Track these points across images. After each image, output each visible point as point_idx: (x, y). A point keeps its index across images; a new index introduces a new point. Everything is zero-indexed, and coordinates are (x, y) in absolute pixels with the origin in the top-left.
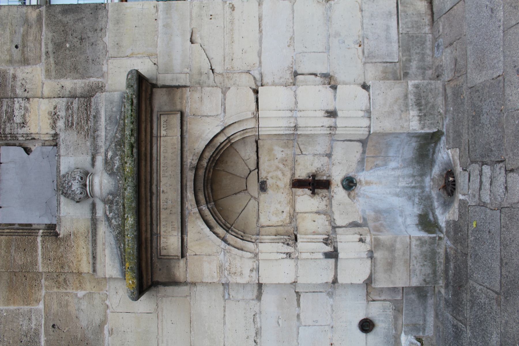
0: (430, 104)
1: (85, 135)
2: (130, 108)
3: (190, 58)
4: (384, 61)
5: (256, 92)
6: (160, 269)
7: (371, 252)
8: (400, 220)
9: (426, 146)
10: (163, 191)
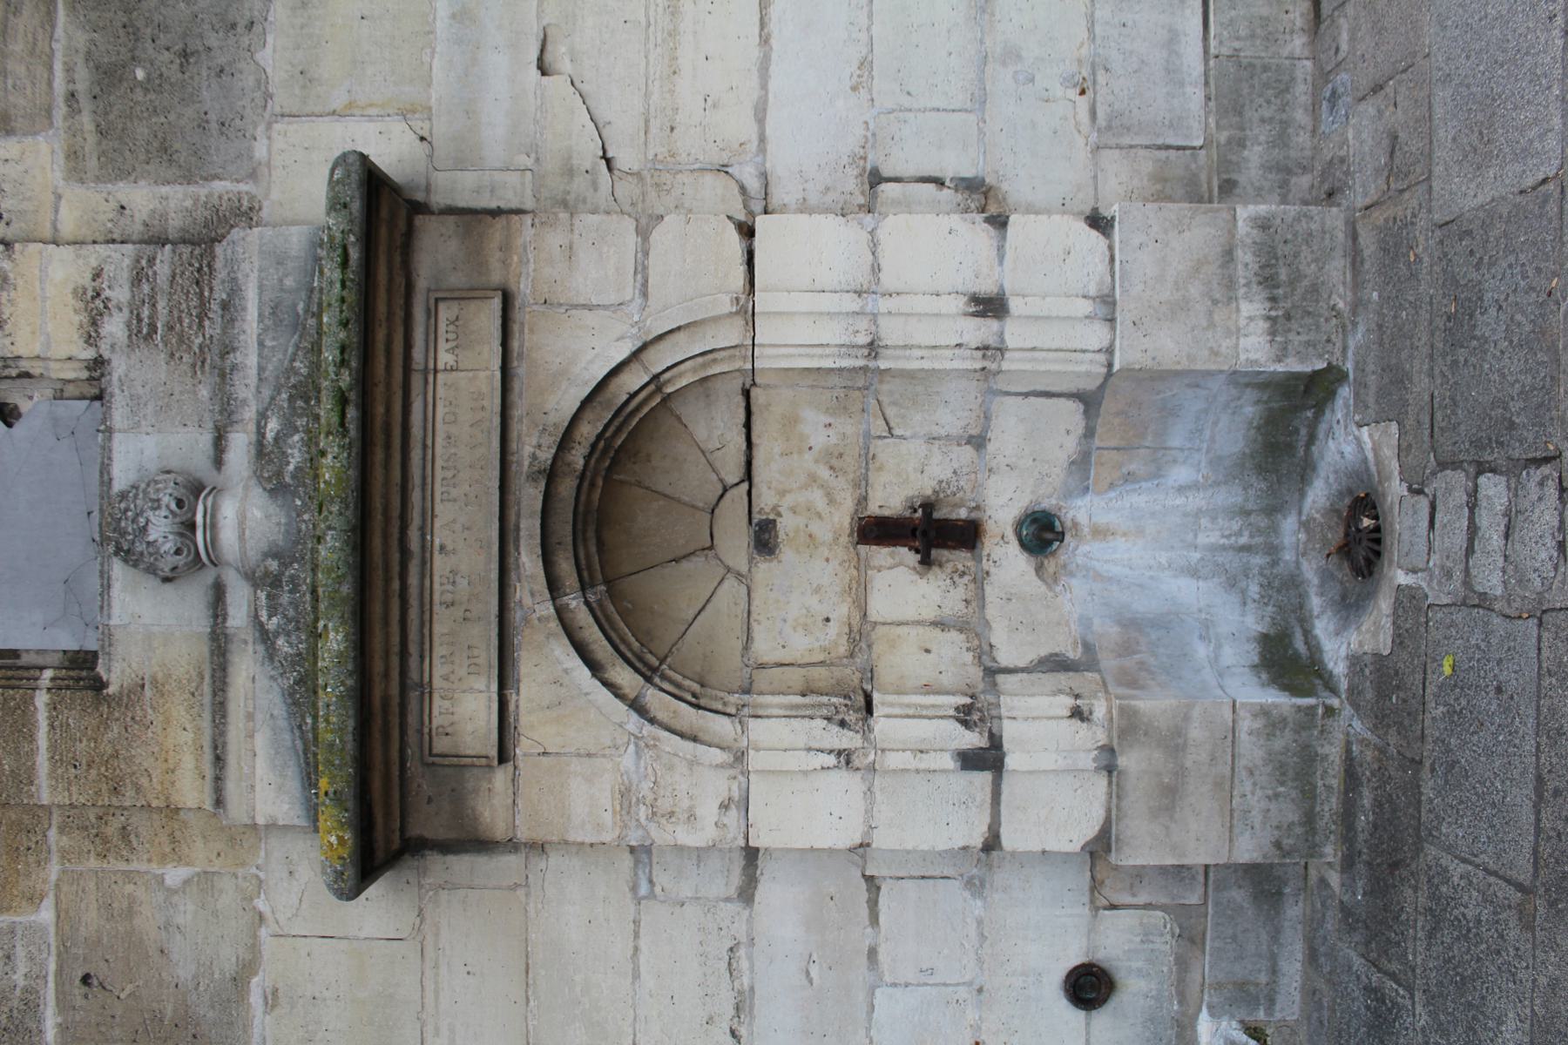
0: (1306, 283)
1: (194, 366)
2: (337, 275)
3: (536, 122)
4: (1160, 142)
5: (747, 232)
6: (430, 800)
7: (1109, 751)
8: (1202, 651)
9: (1290, 409)
10: (442, 548)
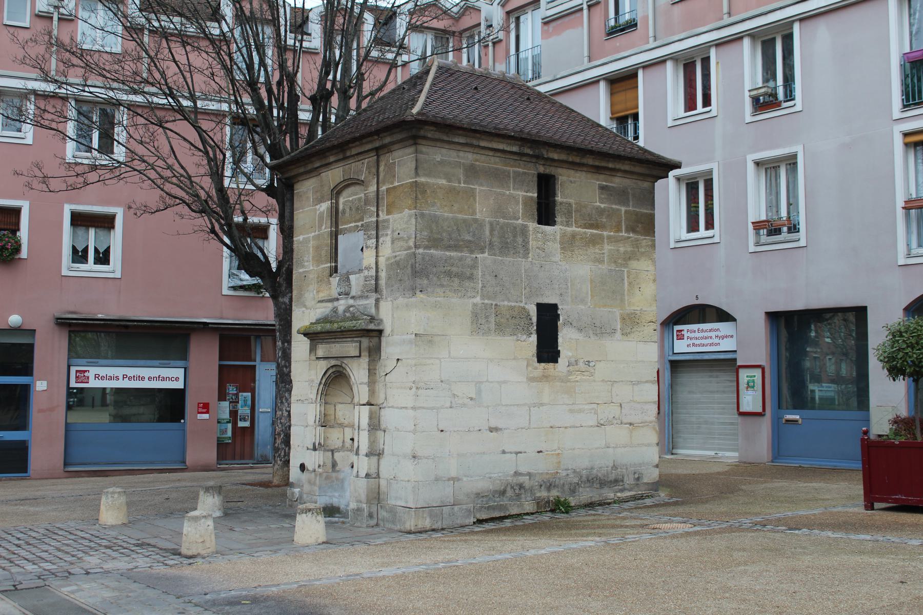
8: (336, 494)
